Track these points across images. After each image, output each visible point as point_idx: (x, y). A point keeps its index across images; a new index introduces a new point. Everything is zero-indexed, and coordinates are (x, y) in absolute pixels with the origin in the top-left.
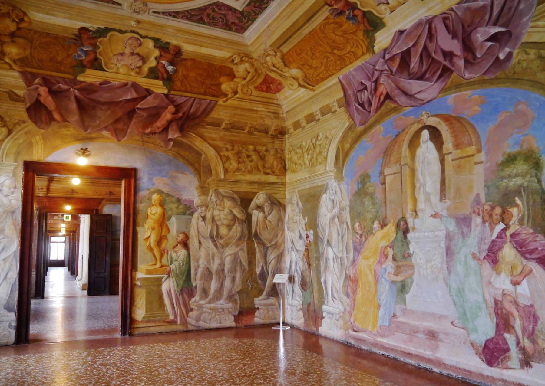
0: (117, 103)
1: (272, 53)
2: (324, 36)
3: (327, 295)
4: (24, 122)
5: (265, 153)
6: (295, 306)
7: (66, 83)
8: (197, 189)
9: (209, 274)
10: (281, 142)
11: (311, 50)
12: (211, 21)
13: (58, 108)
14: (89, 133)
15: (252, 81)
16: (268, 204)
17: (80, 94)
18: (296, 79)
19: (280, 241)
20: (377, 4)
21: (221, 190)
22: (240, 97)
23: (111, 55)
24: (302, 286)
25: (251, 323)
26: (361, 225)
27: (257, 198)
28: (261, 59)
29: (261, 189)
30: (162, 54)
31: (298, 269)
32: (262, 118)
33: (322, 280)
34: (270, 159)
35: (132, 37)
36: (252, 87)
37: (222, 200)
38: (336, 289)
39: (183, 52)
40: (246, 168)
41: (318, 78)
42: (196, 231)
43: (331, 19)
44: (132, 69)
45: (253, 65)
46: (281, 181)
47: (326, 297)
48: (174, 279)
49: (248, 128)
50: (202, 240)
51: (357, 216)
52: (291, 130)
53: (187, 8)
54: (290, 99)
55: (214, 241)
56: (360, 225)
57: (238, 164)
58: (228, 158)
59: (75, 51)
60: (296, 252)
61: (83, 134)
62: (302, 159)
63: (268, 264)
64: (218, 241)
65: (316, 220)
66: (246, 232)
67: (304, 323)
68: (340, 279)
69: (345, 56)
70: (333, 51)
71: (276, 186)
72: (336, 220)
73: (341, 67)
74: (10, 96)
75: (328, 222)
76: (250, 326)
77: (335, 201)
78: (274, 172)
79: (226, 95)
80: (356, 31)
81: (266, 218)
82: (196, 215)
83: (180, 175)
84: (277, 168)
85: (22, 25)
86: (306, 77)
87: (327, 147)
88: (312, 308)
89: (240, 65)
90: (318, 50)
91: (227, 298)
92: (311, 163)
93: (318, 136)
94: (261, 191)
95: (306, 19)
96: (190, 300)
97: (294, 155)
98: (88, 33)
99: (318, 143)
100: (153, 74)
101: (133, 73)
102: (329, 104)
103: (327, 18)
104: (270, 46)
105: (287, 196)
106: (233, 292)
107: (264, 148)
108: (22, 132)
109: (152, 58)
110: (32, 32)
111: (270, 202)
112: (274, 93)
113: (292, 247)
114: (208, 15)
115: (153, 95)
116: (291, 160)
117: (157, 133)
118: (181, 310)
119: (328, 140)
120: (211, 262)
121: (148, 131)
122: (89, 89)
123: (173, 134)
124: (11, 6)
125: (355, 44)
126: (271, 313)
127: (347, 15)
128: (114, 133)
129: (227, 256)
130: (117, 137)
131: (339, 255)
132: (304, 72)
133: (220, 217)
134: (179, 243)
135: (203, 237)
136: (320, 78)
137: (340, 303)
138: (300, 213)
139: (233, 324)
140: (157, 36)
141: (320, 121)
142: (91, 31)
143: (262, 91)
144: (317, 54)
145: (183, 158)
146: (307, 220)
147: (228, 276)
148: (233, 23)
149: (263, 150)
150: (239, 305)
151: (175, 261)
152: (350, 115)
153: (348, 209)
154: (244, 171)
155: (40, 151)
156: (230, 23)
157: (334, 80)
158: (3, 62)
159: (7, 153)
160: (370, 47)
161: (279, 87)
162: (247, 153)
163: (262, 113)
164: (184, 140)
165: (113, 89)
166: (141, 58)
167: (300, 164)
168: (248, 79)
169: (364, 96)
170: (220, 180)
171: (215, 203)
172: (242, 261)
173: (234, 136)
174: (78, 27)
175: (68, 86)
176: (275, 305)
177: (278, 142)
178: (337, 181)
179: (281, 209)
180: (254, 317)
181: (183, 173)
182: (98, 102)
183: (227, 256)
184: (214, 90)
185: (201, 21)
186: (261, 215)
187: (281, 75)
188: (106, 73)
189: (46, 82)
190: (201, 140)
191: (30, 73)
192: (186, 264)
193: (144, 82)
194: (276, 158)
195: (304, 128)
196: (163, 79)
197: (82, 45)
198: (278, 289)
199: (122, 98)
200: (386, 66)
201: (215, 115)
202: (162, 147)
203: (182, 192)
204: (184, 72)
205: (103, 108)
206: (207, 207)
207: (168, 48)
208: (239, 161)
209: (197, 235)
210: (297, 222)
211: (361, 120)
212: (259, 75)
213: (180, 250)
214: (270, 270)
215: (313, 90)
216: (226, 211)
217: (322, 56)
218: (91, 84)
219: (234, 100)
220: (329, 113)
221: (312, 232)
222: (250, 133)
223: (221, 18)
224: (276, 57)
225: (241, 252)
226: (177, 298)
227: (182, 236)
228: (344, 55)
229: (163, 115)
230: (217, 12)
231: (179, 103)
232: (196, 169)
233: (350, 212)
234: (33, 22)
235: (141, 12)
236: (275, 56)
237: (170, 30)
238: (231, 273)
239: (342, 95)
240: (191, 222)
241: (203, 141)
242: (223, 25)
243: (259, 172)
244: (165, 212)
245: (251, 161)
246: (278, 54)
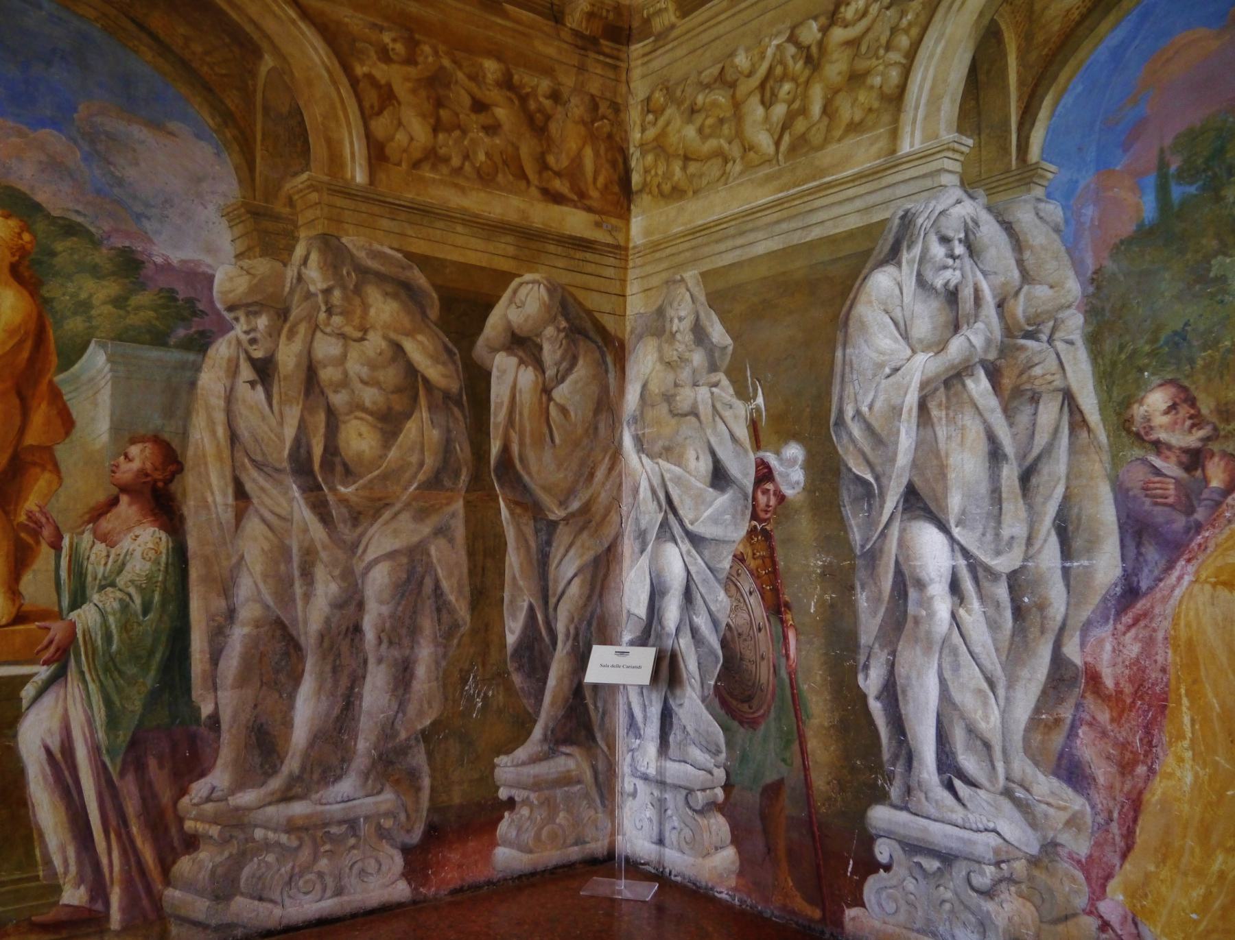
3: (909, 758)
5: (547, 103)
6: (677, 787)
8: (230, 216)
9: (286, 654)
10: (611, 74)
16: (559, 330)
19: (604, 497)
21: (353, 241)
24: (724, 703)
25: (478, 874)
26: (1192, 402)
27: (511, 301)
29: (530, 263)
31: (702, 621)
33: (871, 682)
37: (358, 290)
38: (971, 731)
40: (466, 157)
42: (221, 431)
46: (610, 240)
47: (899, 769)
48: (92, 687)
50: (254, 481)
51: (1153, 354)
55: (312, 489)
56: (1185, 399)
57: (436, 130)
58: (388, 96)
60: (686, 546)
63: (552, 601)
64: (333, 489)
65: (823, 396)
66: (463, 451)
67: (741, 874)
68: (1010, 686)
71: (588, 256)
72: (979, 386)
75: (912, 399)
76: (475, 887)
77: (967, 293)
78: (582, 195)
81: (546, 391)
82: (222, 349)
83: (139, 132)
84: (595, 179)
88: (789, 807)
91: (374, 764)
92: (786, 139)
94: (530, 271)
96: (184, 792)
97: (677, 122)
105: (636, 305)
106: (403, 735)
107: (545, 85)
111: (564, 324)
113: (664, 525)
118: (129, 850)
120: (298, 589)
126: (562, 818)
129: (376, 561)
131: (1004, 564)
133: (346, 374)
134: (124, 489)
135: (258, 466)
137: (1007, 805)
138: (713, 368)
139: (401, 890)
145: (162, 47)
146: (760, 400)
147: (380, 661)
149: (540, 91)
150: (425, 795)
151: (102, 588)
153: (1075, 323)
154: (458, 171)
162: (472, 86)
170: (347, 192)
171: (320, 297)
172: (445, 585)
176: (579, 782)
179: (609, 359)
180: (494, 844)
181: (155, 125)
183: (376, 561)
186: (527, 377)
192: (164, 603)
194: (592, 137)
198: (591, 707)
203: (148, 226)
206: (283, 314)
208: (438, 120)
209: (226, 453)
210: (694, 413)
213: (129, 529)
214: (561, 627)
216: (375, 343)
221: (794, 451)
225: (442, 542)
226: (108, 788)
227: (139, 457)
232: (227, 117)
233: (1094, 341)
238: (391, 643)
240: (193, 384)
243: (523, 184)
244: (49, 320)
245: (492, 129)
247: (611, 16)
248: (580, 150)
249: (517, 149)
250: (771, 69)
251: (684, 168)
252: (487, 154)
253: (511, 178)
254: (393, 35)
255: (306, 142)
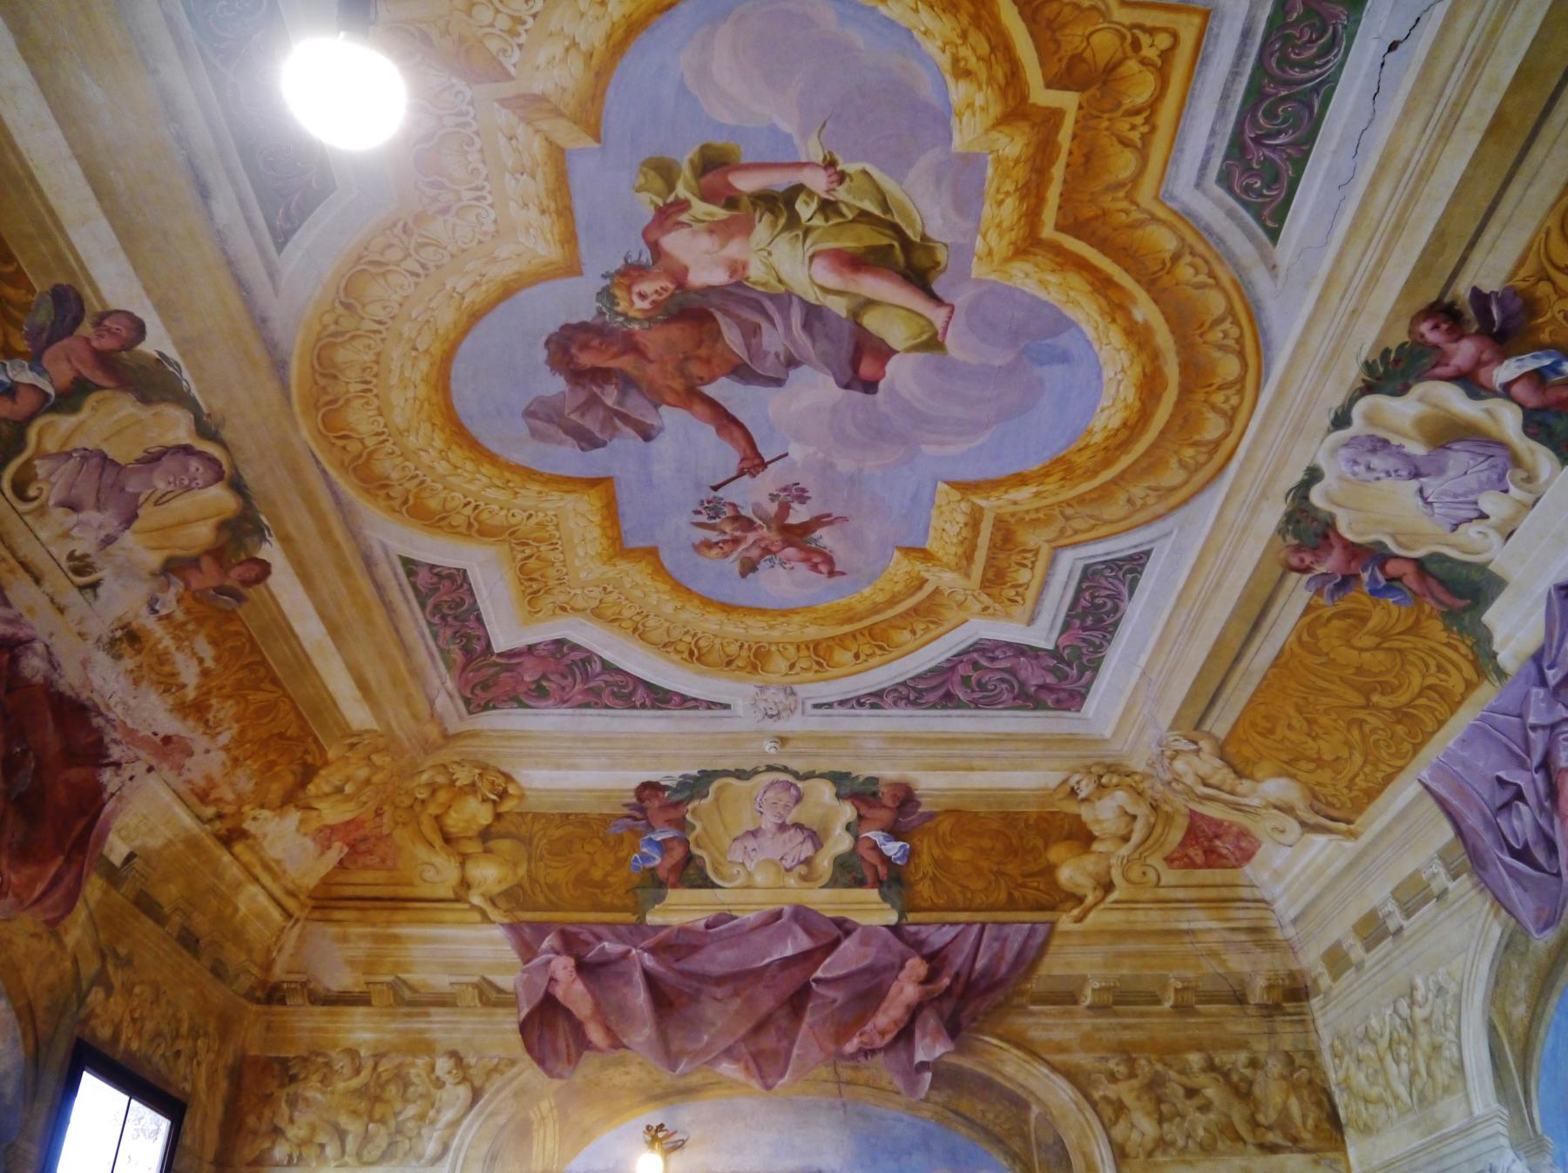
0: (756, 974)
1: (1183, 745)
2: (1323, 659)
4: (513, 1063)
5: (1248, 1072)
7: (619, 938)
10: (1299, 1028)
11: (1299, 710)
12: (977, 695)
13: (599, 1011)
14: (684, 1075)
15: (1150, 842)
17: (657, 962)
18: (1287, 809)
20: (1449, 527)
22: (1124, 896)
23: (727, 841)
28: (1160, 769)
30: (863, 812)
32: (1213, 954)
34: (1273, 1093)
35: (772, 784)
36: (1156, 861)
39: (921, 796)
40: (1189, 1136)
41: (1354, 793)
43: (1324, 606)
44: (788, 870)
45: (1140, 794)
49: (1172, 995)
52: (1325, 981)
53: (900, 675)
54: (1289, 878)
57: (1160, 1122)
58: (1120, 1108)
59: (635, 848)
61: (667, 1078)
62: (1381, 1079)
69: (1415, 707)
70: (1368, 699)
73: (1414, 744)
74: (481, 994)
79: (1080, 900)
80: (1417, 621)
84: (1304, 1124)
85: (506, 807)
86: (1315, 797)
87: (1452, 1024)
89: (1100, 799)
90: (1322, 708)
92: (1414, 1092)
93: (1413, 988)
95: (1247, 628)
97: (1353, 1069)
98: (660, 794)
99: (1420, 1013)
100: (849, 872)
101: (791, 881)
102: (1417, 871)
103: (1308, 609)
104: (1171, 728)
107: (1243, 1057)
108: (503, 1095)
109: (839, 830)
110: (529, 817)
112: (1234, 867)
114: (965, 681)
115: (855, 937)
116: (1346, 1085)
117: (880, 1050)
119: (1449, 997)
121: (851, 1046)
122: (676, 945)
123: (932, 1047)
124: (476, 767)
125: (1432, 664)
127: (1368, 584)
128: (752, 1065)
130: (762, 1077)
132: (1305, 784)
136: (1361, 790)
140: (839, 767)
141: (1406, 933)
142: (665, 788)
143: (1192, 865)
144: (1324, 720)
145: (970, 1122)
148: (1041, 687)
152: (1497, 898)
154: (1184, 1150)
155: (549, 1145)
156: (1033, 689)
157: (1405, 792)
158: (466, 906)
159: (465, 1160)
160: (1484, 660)
161: (1244, 844)
162: (1184, 1079)
163: (1208, 937)
164: (966, 1063)
165: (741, 934)
166: (806, 833)
167: (1381, 1100)
168: (1136, 838)
169: (1522, 823)
173: (1127, 1027)
174: (635, 784)
175: (624, 942)
177: (1288, 1029)
178: (1521, 1153)
182: (703, 978)
184: (1037, 889)
185: (948, 700)
187: (1237, 807)
188: (718, 891)
189: (570, 942)
190: (1020, 1054)
191: (530, 924)
193: (827, 901)
194: (1294, 1087)
195: (1360, 966)
196: (878, 883)
197: (651, 828)
199: (770, 955)
200: (1560, 706)
201: (1054, 967)
202: (898, 1093)
204: (936, 852)
205: (719, 992)
207: (874, 794)
208: (1161, 1114)
211: (1539, 909)
212: (1169, 818)
215: (1352, 835)
217: (1341, 722)
218: (683, 930)
219: (1105, 909)
220: (1426, 901)
222: (1181, 1009)
223: (1002, 680)
224: (1201, 754)
228: (1408, 705)
229: (894, 989)
230: (987, 668)
231: (937, 946)
234: (528, 793)
235: (784, 714)
236: (1198, 752)
237: (871, 744)
239: (1448, 832)
241: (1028, 1058)
242: (1015, 699)
243: (1240, 1145)
245: (1205, 1108)
246: (1205, 745)
247: (1287, 982)
248: (1285, 1103)
249: (1229, 1117)
250: (1391, 1034)
251: (1366, 1109)
252: (1205, 1129)
253: (1229, 1143)
254: (1116, 1060)
255: (1068, 1159)
